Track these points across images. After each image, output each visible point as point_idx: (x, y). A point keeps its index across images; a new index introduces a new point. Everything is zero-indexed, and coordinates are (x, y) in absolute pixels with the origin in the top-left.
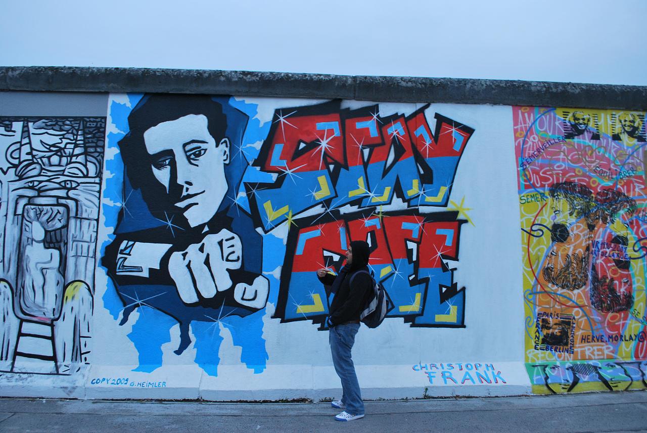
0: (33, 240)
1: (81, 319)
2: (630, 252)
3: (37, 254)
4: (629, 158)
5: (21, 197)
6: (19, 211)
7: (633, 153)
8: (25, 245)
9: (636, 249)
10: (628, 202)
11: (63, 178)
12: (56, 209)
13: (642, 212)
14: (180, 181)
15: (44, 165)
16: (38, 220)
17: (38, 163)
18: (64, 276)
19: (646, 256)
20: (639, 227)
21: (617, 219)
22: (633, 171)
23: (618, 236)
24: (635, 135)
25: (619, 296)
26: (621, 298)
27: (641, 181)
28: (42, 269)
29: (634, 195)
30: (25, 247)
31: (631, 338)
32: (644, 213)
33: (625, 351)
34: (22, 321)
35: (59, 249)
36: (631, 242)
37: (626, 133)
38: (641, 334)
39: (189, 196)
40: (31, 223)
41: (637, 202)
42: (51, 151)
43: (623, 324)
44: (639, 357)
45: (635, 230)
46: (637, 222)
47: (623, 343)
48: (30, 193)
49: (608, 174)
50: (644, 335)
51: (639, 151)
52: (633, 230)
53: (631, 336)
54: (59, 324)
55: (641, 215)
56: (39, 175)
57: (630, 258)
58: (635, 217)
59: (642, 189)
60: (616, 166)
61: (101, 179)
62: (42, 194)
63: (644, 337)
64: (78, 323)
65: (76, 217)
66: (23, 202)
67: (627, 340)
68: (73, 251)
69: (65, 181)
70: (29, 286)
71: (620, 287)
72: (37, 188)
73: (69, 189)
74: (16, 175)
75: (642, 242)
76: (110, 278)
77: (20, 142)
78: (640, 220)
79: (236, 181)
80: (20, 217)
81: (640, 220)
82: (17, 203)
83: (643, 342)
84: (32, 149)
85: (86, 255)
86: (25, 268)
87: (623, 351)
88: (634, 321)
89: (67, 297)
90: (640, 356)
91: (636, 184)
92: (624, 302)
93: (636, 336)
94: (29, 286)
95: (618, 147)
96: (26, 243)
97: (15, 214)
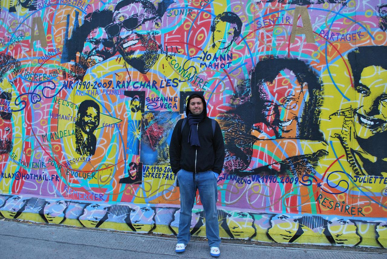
2: (12, 106)
4: (20, 26)
7: (24, 21)
9: (17, 103)
10: (14, 64)
13: (25, 71)
19: (25, 109)
20: (21, 84)
21: (5, 78)
22: (22, 37)
23: (4, 93)
24: (27, 6)
25: (2, 141)
26: (4, 143)
27: (27, 45)
29: (20, 57)
31: (9, 176)
32: (26, 72)
33: (5, 186)
36: (14, 97)
37: (20, 5)
38: (17, 174)
41: (22, 63)
43: (5, 164)
44: (15, 192)
45: (18, 87)
46: (20, 80)
47: (4, 179)
49: (2, 41)
50: (19, 174)
51: (29, 19)
52: (16, 87)
53: (9, 174)
55: (23, 74)
57: (12, 111)
58: (19, 76)
59: (27, 52)
60: (9, 34)
63: (19, 176)
67: (7, 178)
71: (3, 134)
75: (23, 97)
78: (22, 78)
81: (22, 78)
83: (19, 180)
87: (4, 186)
88: (12, 162)
90: (16, 191)
91: (23, 48)
92: (5, 147)
93: (13, 175)
95: (13, 18)
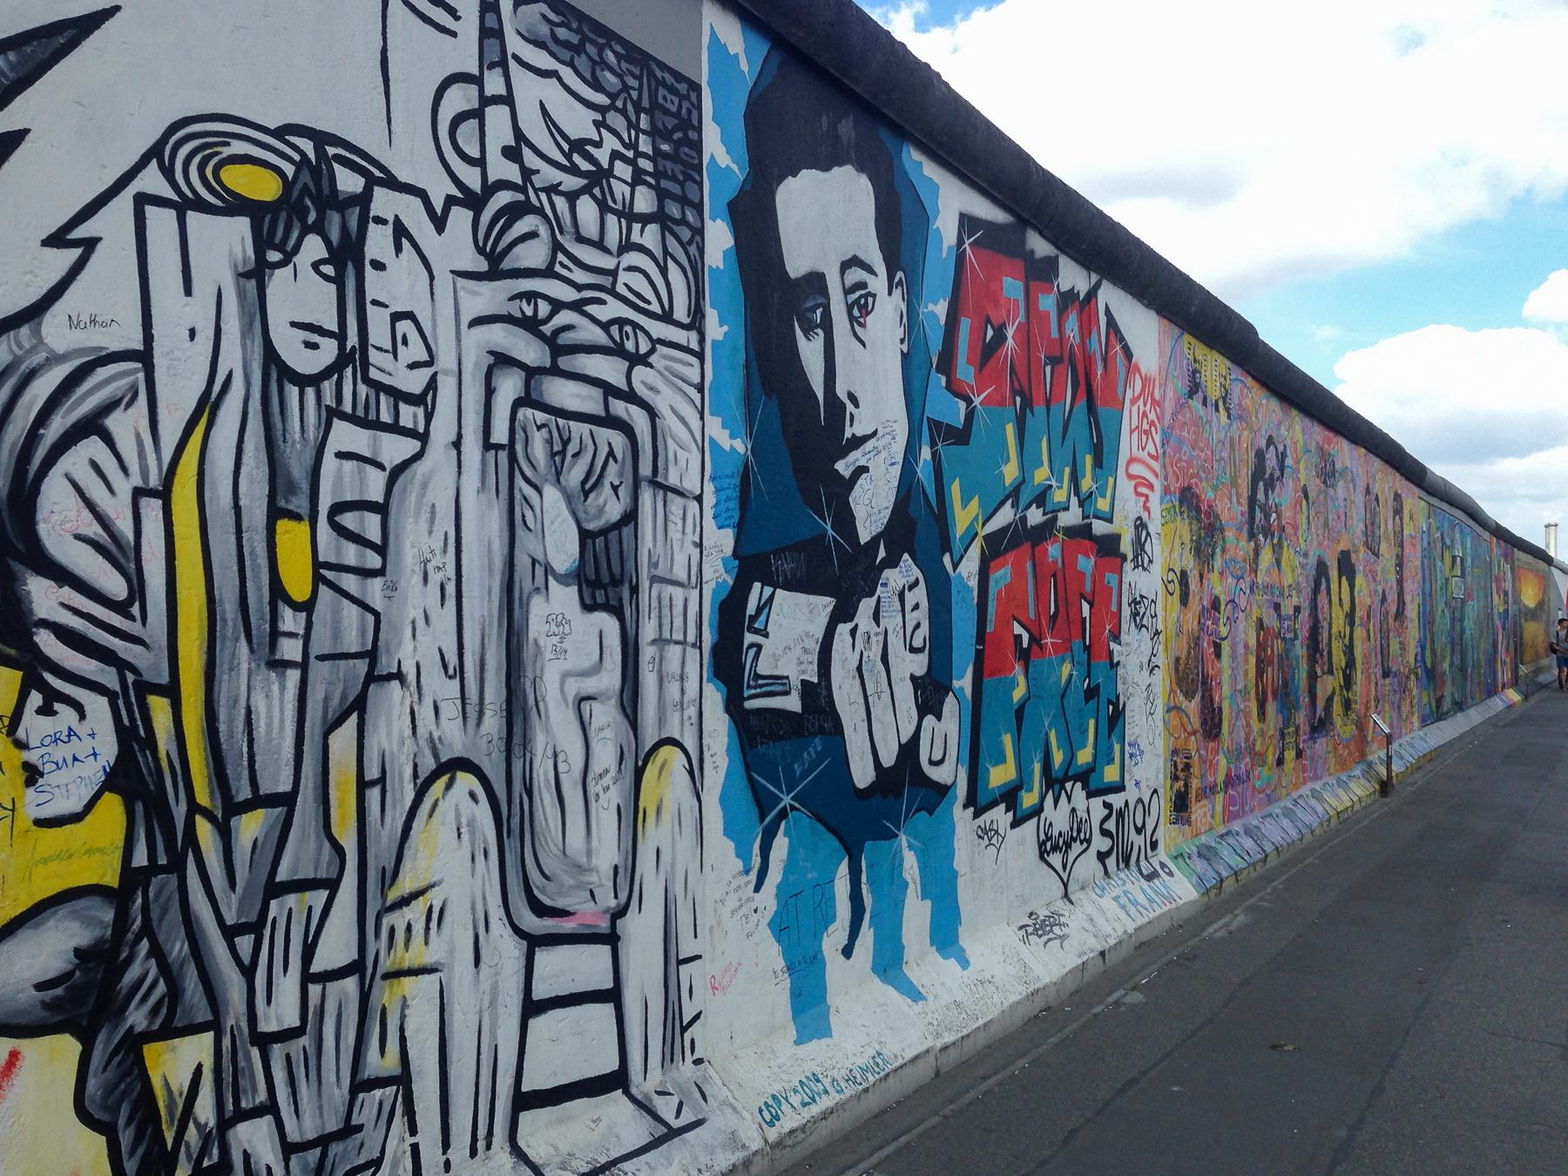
0: (548, 569)
1: (678, 889)
5: (502, 360)
6: (500, 434)
8: (525, 595)
11: (612, 309)
12: (606, 435)
15: (561, 232)
16: (558, 480)
17: (540, 211)
18: (634, 724)
28: (583, 699)
30: (528, 604)
34: (534, 942)
35: (618, 612)
39: (857, 442)
40: (539, 490)
42: (574, 170)
48: (531, 351)
56: (548, 273)
61: (702, 341)
62: (565, 362)
64: (673, 915)
65: (655, 484)
66: (509, 387)
68: (652, 621)
69: (622, 322)
70: (547, 780)
72: (547, 329)
73: (637, 359)
74: (481, 250)
76: (732, 724)
80: (503, 456)
82: (490, 391)
85: (681, 638)
86: (531, 700)
89: (645, 810)
94: (547, 780)
96: (527, 586)
97: (488, 446)
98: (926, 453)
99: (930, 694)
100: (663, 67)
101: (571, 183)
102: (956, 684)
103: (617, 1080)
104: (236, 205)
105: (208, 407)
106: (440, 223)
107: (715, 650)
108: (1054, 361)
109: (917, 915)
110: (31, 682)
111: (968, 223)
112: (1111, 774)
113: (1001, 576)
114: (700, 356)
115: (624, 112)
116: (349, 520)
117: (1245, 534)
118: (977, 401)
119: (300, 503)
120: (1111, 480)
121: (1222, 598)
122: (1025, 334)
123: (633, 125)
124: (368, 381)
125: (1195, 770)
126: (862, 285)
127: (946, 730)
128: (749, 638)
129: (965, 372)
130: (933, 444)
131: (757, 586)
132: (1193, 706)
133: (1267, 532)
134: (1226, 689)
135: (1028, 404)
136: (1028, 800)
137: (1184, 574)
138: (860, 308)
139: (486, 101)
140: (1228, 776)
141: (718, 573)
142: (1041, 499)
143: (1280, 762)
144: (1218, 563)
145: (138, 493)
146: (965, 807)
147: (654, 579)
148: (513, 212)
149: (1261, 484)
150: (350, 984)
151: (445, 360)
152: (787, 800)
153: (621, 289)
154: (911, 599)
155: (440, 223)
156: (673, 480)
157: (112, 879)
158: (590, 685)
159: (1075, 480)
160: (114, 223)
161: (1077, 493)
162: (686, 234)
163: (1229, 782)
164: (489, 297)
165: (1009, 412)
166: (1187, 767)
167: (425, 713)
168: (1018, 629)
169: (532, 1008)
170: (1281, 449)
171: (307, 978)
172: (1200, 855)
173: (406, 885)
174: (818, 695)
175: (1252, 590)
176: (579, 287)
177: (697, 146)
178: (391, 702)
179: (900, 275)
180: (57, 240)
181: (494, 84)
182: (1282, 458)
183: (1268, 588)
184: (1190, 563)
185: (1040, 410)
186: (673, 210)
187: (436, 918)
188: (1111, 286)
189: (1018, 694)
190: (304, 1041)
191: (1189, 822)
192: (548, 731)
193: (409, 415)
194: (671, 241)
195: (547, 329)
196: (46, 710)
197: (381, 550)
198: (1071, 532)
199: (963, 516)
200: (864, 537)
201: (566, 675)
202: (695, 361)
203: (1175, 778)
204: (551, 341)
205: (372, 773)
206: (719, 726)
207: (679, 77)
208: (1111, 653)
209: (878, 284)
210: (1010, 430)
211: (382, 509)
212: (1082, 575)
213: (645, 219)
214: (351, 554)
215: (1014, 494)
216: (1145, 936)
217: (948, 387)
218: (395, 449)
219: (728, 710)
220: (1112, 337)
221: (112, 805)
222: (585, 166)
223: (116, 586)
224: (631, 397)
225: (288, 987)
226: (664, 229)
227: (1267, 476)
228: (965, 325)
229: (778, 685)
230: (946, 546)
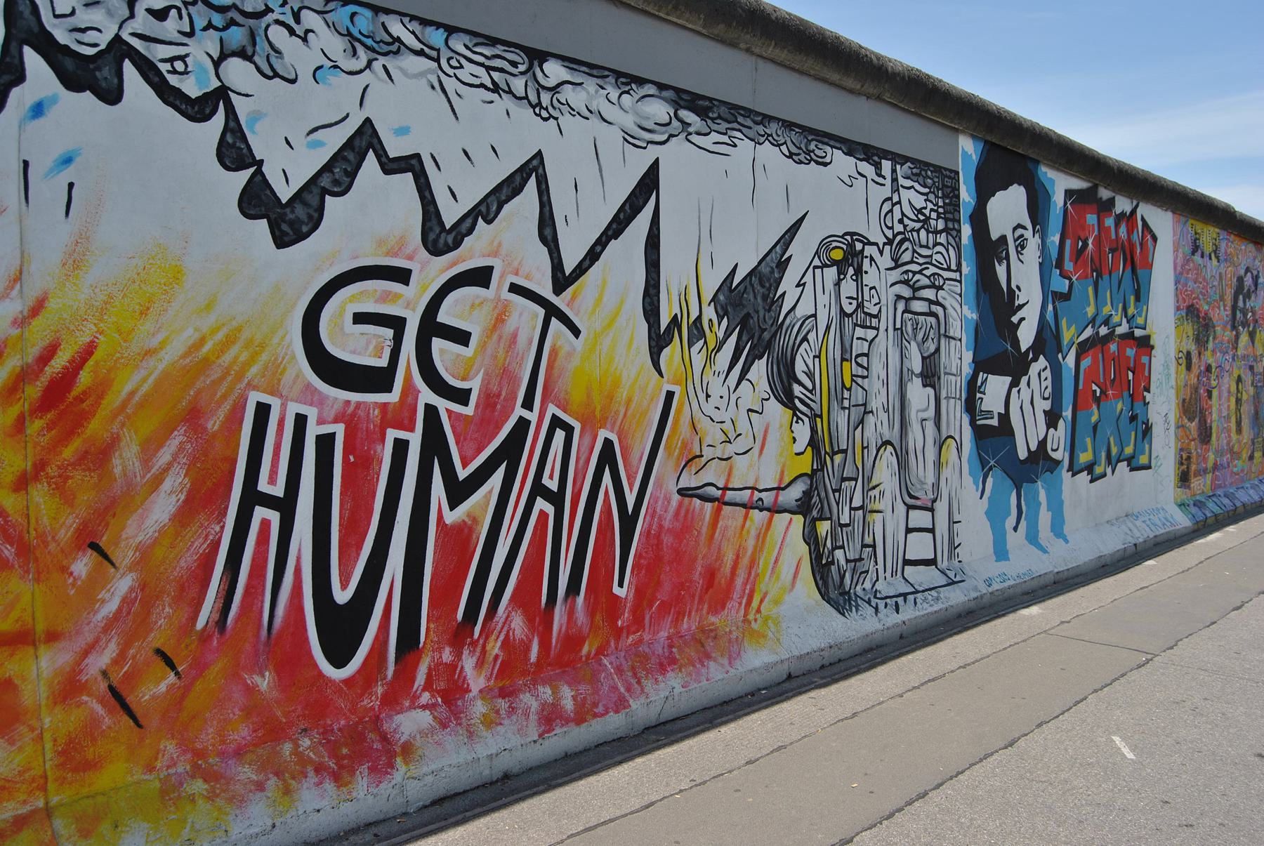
0: (913, 372)
1: (953, 494)
3: (919, 395)
5: (899, 297)
6: (898, 326)
11: (932, 270)
14: (1014, 286)
18: (939, 430)
34: (910, 507)
39: (1021, 307)
42: (919, 221)
48: (906, 292)
54: (937, 505)
56: (912, 262)
61: (961, 276)
65: (946, 336)
66: (901, 306)
69: (934, 274)
72: (911, 283)
73: (940, 288)
74: (892, 259)
77: (890, 199)
79: (1047, 289)
80: (899, 332)
82: (895, 309)
84: (903, 214)
97: (895, 329)
98: (1050, 307)
99: (1052, 419)
100: (946, 169)
101: (918, 225)
102: (1064, 414)
103: (931, 562)
104: (834, 263)
105: (828, 328)
106: (881, 253)
107: (966, 400)
108: (1112, 250)
109: (1045, 517)
110: (794, 414)
111: (1069, 193)
112: (1143, 460)
113: (1086, 363)
114: (960, 282)
115: (934, 193)
116: (859, 360)
117: (1229, 327)
118: (1074, 279)
119: (848, 356)
120: (1145, 307)
121: (1214, 365)
122: (1098, 241)
123: (937, 197)
124: (865, 313)
125: (1194, 460)
126: (1022, 236)
127: (1059, 436)
128: (978, 395)
129: (1068, 266)
130: (1054, 303)
131: (981, 373)
132: (1193, 426)
133: (1245, 324)
134: (1215, 416)
135: (1100, 275)
136: (1098, 470)
137: (1189, 354)
138: (1021, 246)
139: (893, 205)
140: (1215, 464)
141: (967, 370)
142: (1106, 322)
143: (1251, 458)
144: (1210, 345)
145: (814, 357)
146: (1068, 471)
147: (946, 373)
148: (901, 243)
149: (1241, 297)
150: (861, 512)
151: (883, 302)
152: (992, 463)
153: (934, 262)
154: (1043, 375)
155: (881, 253)
156: (951, 334)
157: (809, 472)
158: (925, 415)
159: (1125, 310)
160: (808, 278)
161: (1126, 317)
162: (954, 233)
163: (1216, 467)
164: (895, 275)
165: (1090, 281)
166: (1189, 458)
167: (879, 424)
168: (1094, 387)
169: (909, 531)
170: (1255, 273)
171: (851, 509)
172: (1194, 505)
173: (874, 483)
174: (1005, 418)
175: (1233, 359)
176: (921, 265)
177: (958, 197)
178: (870, 419)
179: (1038, 227)
180: (798, 285)
181: (895, 199)
182: (1256, 279)
183: (1244, 357)
184: (1193, 348)
185: (1106, 277)
186: (950, 225)
187: (882, 494)
188: (1144, 205)
189: (1094, 418)
190: (850, 528)
191: (1189, 487)
192: (913, 432)
193: (874, 322)
194: (950, 237)
195: (911, 283)
196: (797, 422)
197: (867, 369)
198: (1122, 336)
199: (1067, 334)
200: (1023, 349)
201: (918, 411)
202: (958, 284)
203: (1181, 464)
204: (912, 287)
205: (865, 445)
206: (968, 433)
207: (951, 171)
208: (1144, 398)
209: (1028, 234)
210: (1091, 290)
211: (867, 355)
212: (1129, 358)
213: (941, 232)
214: (860, 371)
215: (1093, 321)
216: (1158, 540)
217: (1061, 275)
218: (871, 334)
219: (971, 425)
220: (1145, 232)
221: (809, 448)
222: (922, 218)
223: (811, 388)
224: (937, 303)
225: (847, 509)
226: (948, 233)
227: (1245, 291)
228: (1068, 243)
229: (989, 414)
230: (1060, 350)
